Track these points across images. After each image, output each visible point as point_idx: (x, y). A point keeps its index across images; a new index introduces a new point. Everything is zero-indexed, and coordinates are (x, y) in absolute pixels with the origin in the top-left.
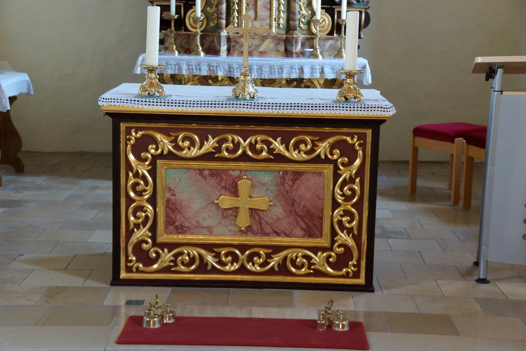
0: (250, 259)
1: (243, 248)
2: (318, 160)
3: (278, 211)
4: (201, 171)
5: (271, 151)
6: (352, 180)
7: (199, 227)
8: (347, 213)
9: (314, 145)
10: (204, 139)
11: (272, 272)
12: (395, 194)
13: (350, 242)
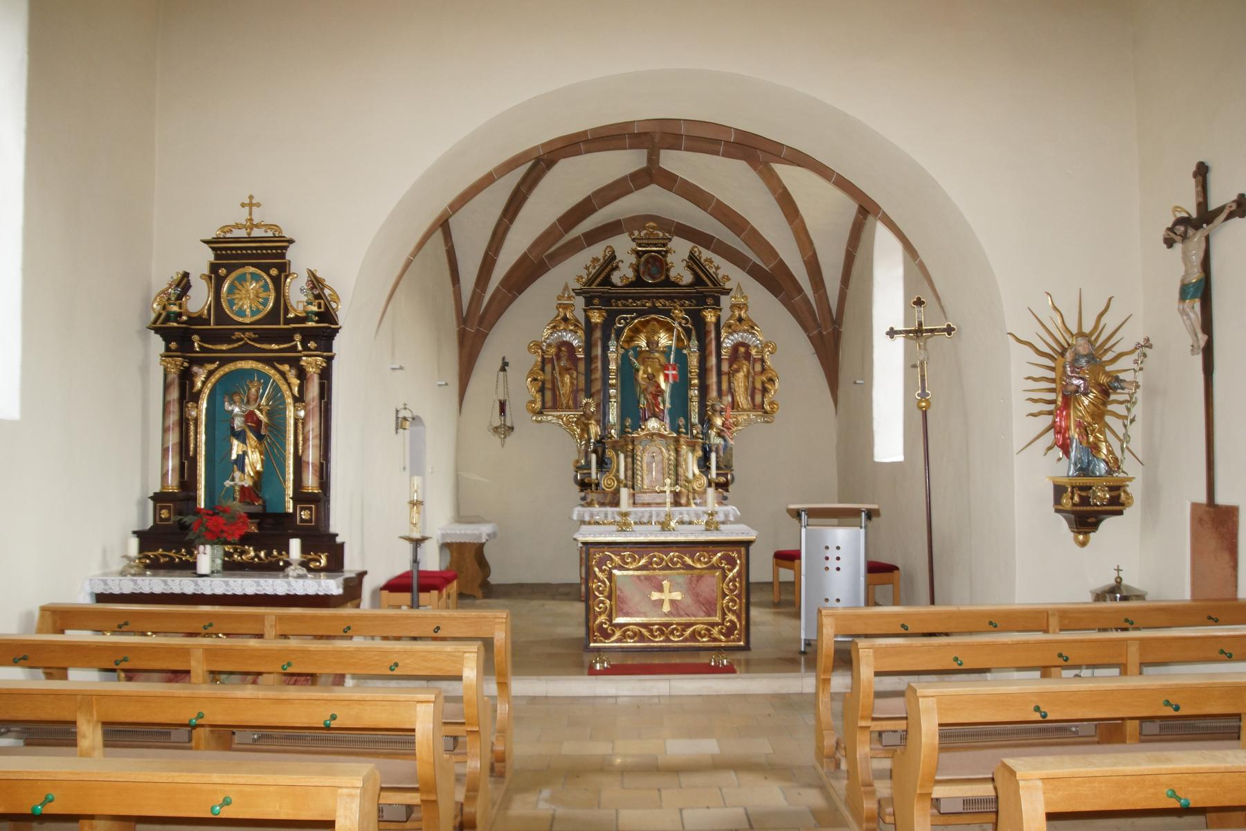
0: (672, 633)
1: (667, 625)
2: (713, 567)
3: (689, 600)
4: (638, 577)
5: (684, 563)
6: (733, 580)
7: (638, 614)
8: (732, 600)
9: (710, 559)
10: (641, 557)
11: (685, 640)
12: (761, 605)
13: (734, 618)
